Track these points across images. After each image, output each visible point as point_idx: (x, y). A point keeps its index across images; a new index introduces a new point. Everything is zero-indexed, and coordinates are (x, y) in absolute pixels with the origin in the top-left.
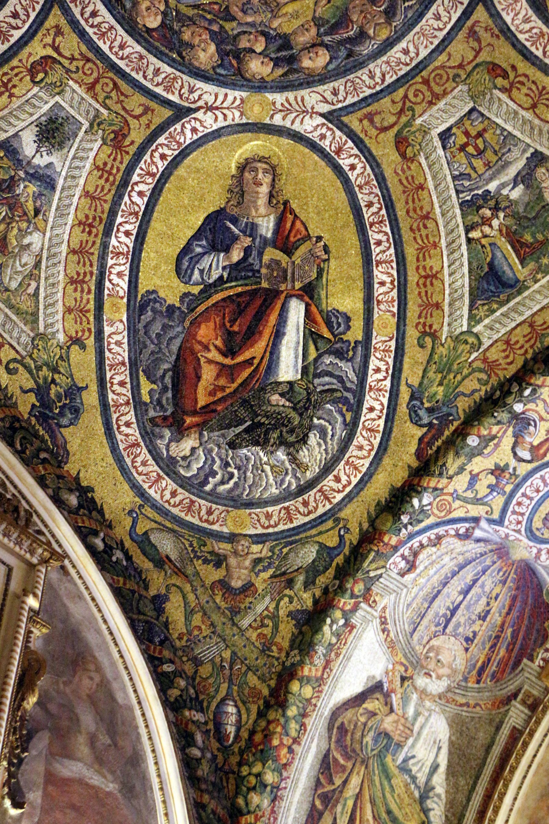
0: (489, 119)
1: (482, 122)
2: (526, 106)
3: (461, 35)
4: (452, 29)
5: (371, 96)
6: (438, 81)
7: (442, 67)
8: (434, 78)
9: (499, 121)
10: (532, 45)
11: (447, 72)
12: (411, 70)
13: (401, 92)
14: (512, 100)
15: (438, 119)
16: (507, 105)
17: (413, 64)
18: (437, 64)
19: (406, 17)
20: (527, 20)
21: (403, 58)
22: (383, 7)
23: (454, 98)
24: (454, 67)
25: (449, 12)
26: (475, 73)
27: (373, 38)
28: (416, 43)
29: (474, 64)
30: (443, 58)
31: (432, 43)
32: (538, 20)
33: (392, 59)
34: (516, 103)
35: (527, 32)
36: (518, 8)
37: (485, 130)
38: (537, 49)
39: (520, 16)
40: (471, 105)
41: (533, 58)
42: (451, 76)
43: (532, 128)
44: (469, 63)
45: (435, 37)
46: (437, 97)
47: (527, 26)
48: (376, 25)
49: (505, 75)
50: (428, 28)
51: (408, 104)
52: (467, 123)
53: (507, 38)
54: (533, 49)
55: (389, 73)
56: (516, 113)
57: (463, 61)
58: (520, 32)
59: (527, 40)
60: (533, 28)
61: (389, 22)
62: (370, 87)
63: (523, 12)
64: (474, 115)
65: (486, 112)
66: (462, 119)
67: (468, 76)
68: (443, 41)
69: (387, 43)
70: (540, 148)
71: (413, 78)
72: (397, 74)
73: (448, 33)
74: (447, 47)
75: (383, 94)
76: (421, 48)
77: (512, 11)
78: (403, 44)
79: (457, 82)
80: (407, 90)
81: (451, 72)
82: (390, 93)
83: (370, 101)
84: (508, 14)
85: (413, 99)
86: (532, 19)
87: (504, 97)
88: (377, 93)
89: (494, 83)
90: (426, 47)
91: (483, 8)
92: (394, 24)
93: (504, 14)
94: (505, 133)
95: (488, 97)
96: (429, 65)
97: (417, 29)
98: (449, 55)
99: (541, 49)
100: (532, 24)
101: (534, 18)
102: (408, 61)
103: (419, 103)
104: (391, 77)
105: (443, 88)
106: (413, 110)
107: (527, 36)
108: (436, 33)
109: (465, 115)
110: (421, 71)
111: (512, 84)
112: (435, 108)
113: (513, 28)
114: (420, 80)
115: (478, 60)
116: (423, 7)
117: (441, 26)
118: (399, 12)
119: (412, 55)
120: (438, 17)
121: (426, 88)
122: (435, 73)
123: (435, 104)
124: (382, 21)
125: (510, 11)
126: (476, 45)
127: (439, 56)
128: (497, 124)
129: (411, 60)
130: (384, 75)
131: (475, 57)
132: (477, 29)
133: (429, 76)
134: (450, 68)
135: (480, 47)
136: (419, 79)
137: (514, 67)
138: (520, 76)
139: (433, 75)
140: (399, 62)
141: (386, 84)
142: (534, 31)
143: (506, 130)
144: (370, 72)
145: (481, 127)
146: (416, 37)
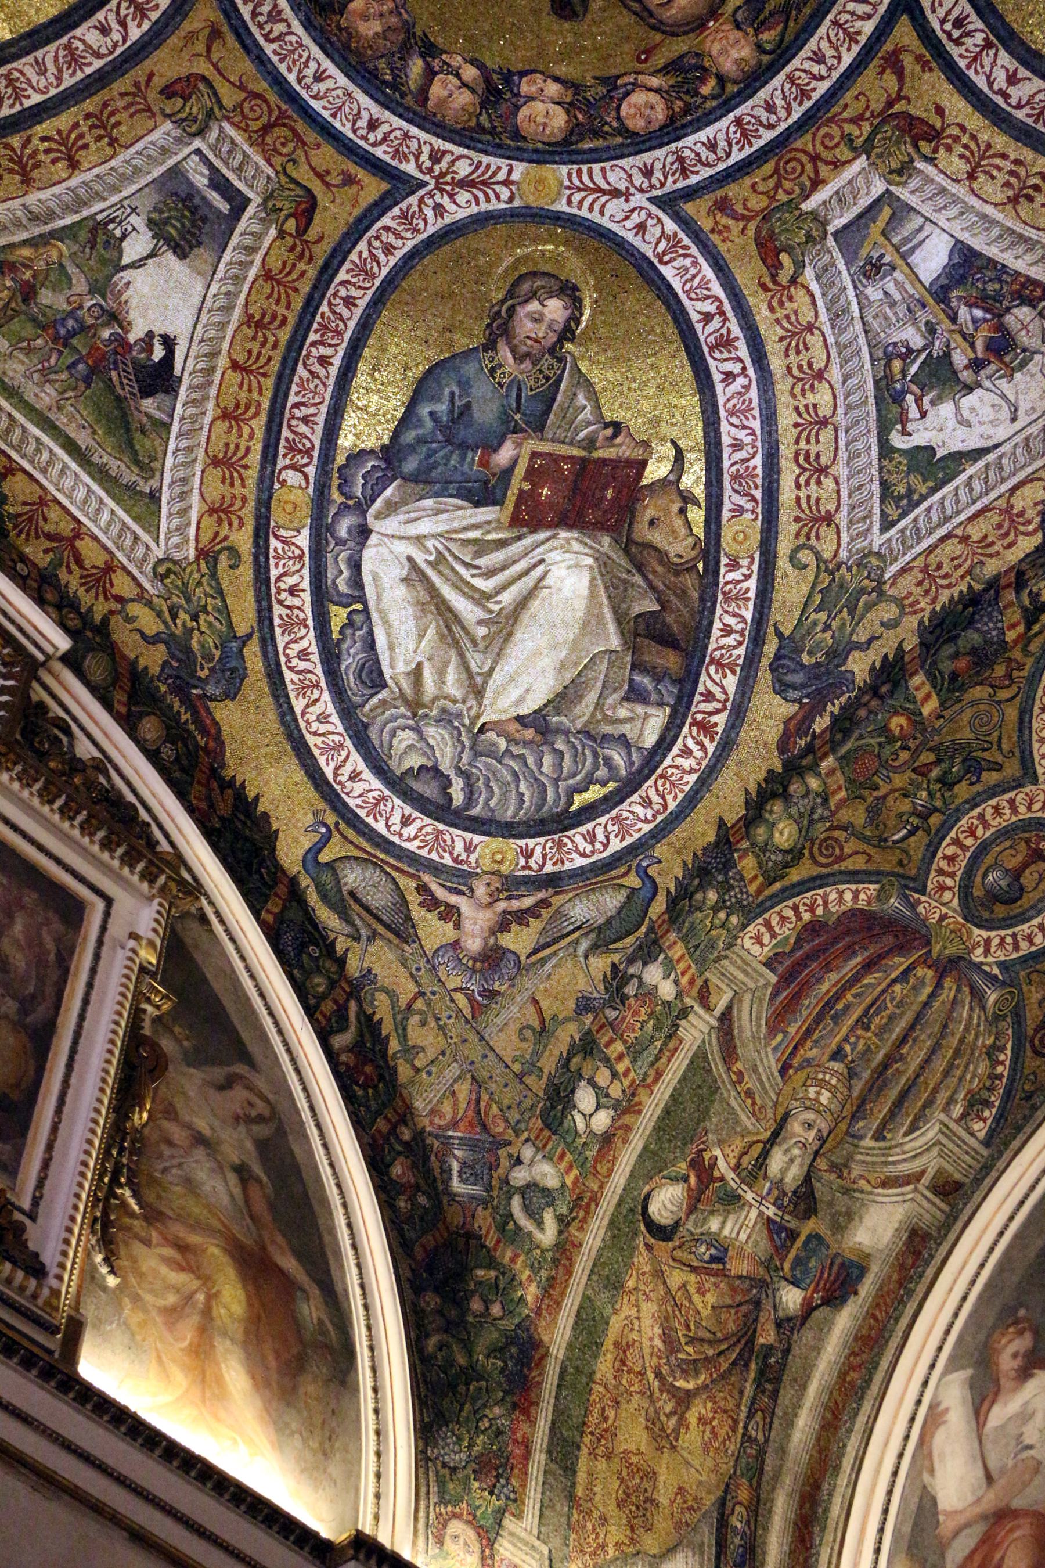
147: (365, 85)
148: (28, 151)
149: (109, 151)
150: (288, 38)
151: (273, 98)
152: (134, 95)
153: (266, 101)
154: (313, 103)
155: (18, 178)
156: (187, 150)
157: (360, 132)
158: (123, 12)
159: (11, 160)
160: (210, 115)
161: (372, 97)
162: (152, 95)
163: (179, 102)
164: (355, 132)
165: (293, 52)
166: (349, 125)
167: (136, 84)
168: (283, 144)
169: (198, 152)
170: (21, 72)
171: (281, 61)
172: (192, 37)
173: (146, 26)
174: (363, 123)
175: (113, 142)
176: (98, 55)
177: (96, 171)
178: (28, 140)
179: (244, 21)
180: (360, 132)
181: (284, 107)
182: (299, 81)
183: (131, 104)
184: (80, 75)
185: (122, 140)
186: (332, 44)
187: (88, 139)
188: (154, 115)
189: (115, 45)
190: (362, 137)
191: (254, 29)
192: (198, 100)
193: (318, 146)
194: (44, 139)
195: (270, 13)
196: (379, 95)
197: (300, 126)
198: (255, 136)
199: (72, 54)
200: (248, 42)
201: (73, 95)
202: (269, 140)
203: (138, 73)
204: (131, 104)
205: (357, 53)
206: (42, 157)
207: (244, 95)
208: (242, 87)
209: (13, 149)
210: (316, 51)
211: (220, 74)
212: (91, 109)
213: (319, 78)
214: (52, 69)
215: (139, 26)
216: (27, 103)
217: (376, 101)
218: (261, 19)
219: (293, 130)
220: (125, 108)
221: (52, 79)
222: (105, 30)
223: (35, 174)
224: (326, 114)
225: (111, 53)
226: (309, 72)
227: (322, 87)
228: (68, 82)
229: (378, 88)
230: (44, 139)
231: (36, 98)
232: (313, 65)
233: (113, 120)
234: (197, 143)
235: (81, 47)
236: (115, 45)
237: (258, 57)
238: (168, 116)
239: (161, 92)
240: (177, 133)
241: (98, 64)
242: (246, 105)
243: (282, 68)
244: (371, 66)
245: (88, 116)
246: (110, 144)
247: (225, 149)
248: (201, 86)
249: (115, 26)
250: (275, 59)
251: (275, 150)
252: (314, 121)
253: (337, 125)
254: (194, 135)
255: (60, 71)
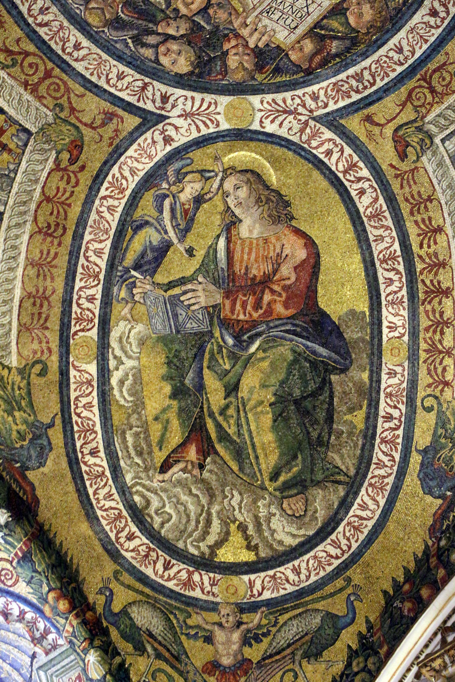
0: (23, 153)
1: (18, 146)
2: (46, 190)
3: (106, 106)
4: (111, 94)
5: (20, 13)
6: (52, 87)
7: (68, 90)
8: (54, 83)
9: (24, 164)
10: (109, 183)
11: (63, 95)
12: (59, 56)
13: (31, 48)
14: (49, 173)
15: (10, 95)
16: (43, 170)
17: (65, 57)
18: (71, 84)
19: (116, 42)
20: (133, 172)
21: (70, 45)
22: (122, 16)
23: (37, 109)
24: (70, 103)
25: (127, 88)
26: (69, 127)
27: (86, 8)
28: (88, 57)
29: (78, 124)
30: (80, 90)
31: (92, 74)
32: (135, 183)
33: (67, 32)
34: (47, 179)
35: (121, 174)
36: (143, 160)
37: (10, 151)
38: (107, 189)
39: (136, 164)
40: (34, 130)
41: (97, 187)
42: (58, 102)
43: (25, 202)
44: (77, 118)
45: (100, 78)
46: (34, 91)
47: (127, 173)
48: (102, 9)
49: (72, 161)
50: (108, 68)
51: (19, 58)
52: (13, 130)
53: (111, 155)
54: (106, 185)
55: (50, 30)
56: (36, 181)
57: (79, 112)
58: (120, 168)
59: (114, 175)
60: (127, 180)
61: (109, 24)
62: (29, 10)
63: (140, 166)
64: (23, 136)
65: (29, 148)
66: (16, 122)
67: (65, 121)
68: (96, 86)
69: (84, 24)
70: (6, 216)
71: (51, 60)
72: (50, 40)
73: (105, 91)
74: (90, 91)
75: (25, 27)
76: (84, 63)
77: (139, 154)
78: (85, 43)
79: (54, 109)
80: (34, 54)
81: (64, 101)
82: (28, 36)
83: (14, 12)
84: (136, 151)
85: (26, 64)
86: (135, 177)
87: (50, 164)
88: (25, 20)
89: (62, 150)
90: (87, 69)
91: (136, 124)
92: (106, 30)
93: (135, 146)
94: (12, 175)
95: (46, 146)
96: (67, 74)
97: (105, 56)
98: (83, 96)
99: (108, 193)
100: (130, 179)
101: (137, 179)
102: (68, 50)
103: (23, 70)
104: (46, 34)
105: (45, 95)
106: (13, 65)
107: (118, 175)
108: (103, 78)
109: (20, 125)
110: (58, 66)
111: (65, 169)
112: (22, 91)
113: (122, 159)
114: (48, 68)
115: (82, 127)
116: (129, 59)
117: (111, 82)
118: (120, 33)
119: (75, 54)
120: (121, 76)
121: (42, 75)
122: (60, 83)
123: (26, 89)
124: (108, 16)
125: (139, 152)
126: (98, 122)
127: (79, 84)
128: (20, 163)
129: (70, 54)
130: (46, 25)
131: (86, 125)
132: (115, 121)
133: (55, 77)
134: (69, 98)
135: (97, 127)
136: (50, 65)
137: (83, 168)
138: (76, 176)
139: (58, 81)
140: (64, 41)
141: (38, 29)
142: (124, 182)
143: (16, 174)
144: (47, 9)
145: (12, 146)
146: (95, 56)
147: (406, 18)
148: (427, 260)
149: (435, 203)
150: (373, 70)
151: (412, 84)
152: (403, 179)
153: (413, 89)
154: (417, 55)
155: (441, 270)
156: (442, 149)
157: (439, 23)
158: (352, 178)
159: (430, 272)
160: (419, 129)
161: (414, 13)
162: (404, 166)
163: (410, 149)
164: (438, 27)
165: (382, 67)
166: (433, 31)
167: (397, 176)
168: (444, 79)
169: (443, 141)
170: (380, 252)
171: (388, 76)
172: (370, 135)
173: (361, 164)
174: (432, 21)
175: (430, 199)
176: (376, 200)
177: (446, 215)
178: (420, 257)
179: (362, 99)
180: (439, 23)
181: (418, 76)
182: (402, 64)
183: (408, 181)
184: (387, 214)
185: (430, 193)
186: (377, 40)
187: (425, 217)
188: (416, 168)
189: (371, 186)
190: (442, 22)
191: (367, 93)
192: (409, 136)
193: (447, 54)
194: (421, 247)
195: (357, 81)
196: (413, 8)
197: (432, 66)
198: (437, 99)
199: (374, 216)
200: (374, 98)
201: (398, 222)
202: (439, 89)
203: (389, 173)
204: (408, 181)
205: (384, 22)
206: (431, 251)
207: (409, 103)
208: (403, 105)
209: (424, 269)
210: (382, 51)
211: (394, 118)
212: (408, 210)
213: (400, 50)
214: (380, 232)
215: (361, 169)
216: (399, 253)
217: (417, 10)
218: (361, 87)
219: (434, 71)
220: (410, 187)
221: (387, 233)
222: (362, 192)
223: (441, 258)
224: (425, 47)
225: (376, 190)
226: (396, 57)
227: (406, 48)
228: (389, 223)
229: (408, 9)
230: (421, 247)
231: (397, 246)
232: (391, 54)
233: (416, 197)
234: (437, 140)
235: (370, 209)
236: (371, 186)
237: (385, 91)
238: (418, 157)
239: (403, 161)
240: (429, 153)
241: (381, 200)
242: (415, 104)
243: (393, 75)
244: (393, 13)
245: (412, 213)
246: (431, 202)
247: (443, 121)
248: (401, 133)
249: (360, 185)
250: (386, 80)
251: (447, 86)
252: (429, 56)
253: (432, 39)
254: (432, 142)
255: (382, 226)
